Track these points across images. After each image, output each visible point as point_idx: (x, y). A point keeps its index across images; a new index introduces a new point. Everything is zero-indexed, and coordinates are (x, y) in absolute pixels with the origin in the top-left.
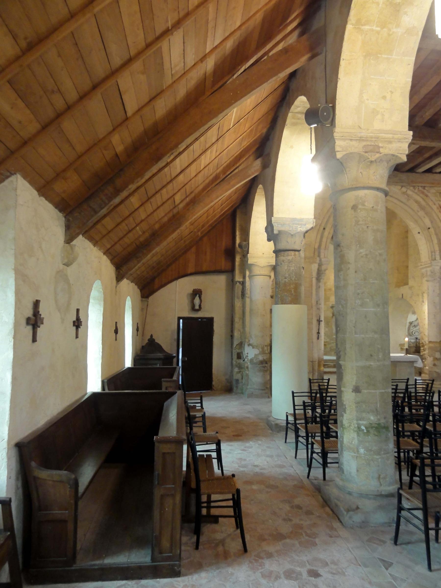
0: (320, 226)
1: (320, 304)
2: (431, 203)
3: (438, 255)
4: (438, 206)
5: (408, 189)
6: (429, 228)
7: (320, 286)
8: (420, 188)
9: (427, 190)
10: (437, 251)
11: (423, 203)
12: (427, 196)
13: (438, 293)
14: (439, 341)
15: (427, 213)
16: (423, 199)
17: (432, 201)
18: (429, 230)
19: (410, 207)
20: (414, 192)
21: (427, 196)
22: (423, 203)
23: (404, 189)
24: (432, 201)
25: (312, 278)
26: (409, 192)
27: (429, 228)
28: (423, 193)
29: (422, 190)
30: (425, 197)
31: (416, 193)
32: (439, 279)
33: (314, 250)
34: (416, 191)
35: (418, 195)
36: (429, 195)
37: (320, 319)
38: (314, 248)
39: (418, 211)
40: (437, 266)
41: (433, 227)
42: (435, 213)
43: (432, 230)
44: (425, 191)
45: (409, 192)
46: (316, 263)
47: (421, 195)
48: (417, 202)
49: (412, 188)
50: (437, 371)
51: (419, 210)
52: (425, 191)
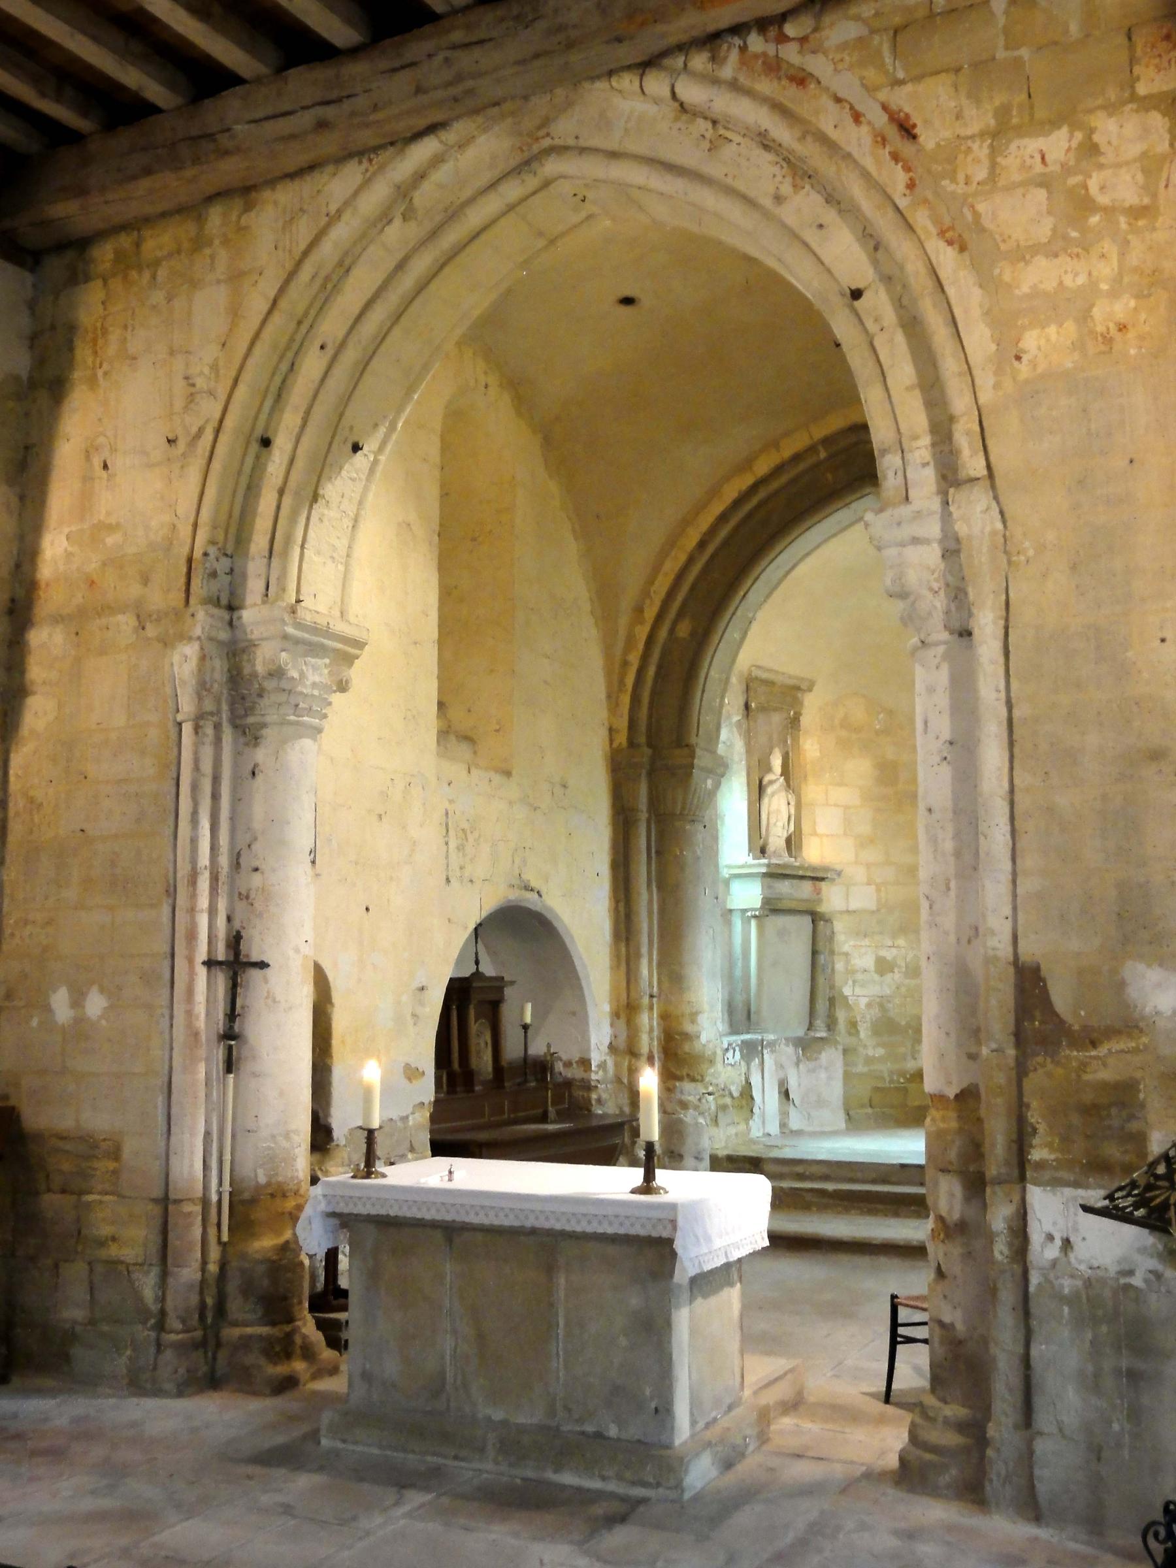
0: (217, 431)
1: (256, 870)
2: (829, 120)
3: (925, 465)
4: (881, 119)
5: (675, 73)
6: (856, 294)
7: (256, 766)
8: (756, 43)
9: (803, 40)
10: (916, 438)
11: (782, 133)
12: (801, 79)
13: (946, 735)
14: (951, 1092)
15: (831, 199)
16: (780, 109)
17: (838, 100)
18: (857, 304)
19: (730, 191)
20: (716, 81)
21: (801, 79)
22: (782, 133)
23: (657, 84)
24: (838, 100)
25: (180, 724)
26: (692, 92)
27: (856, 294)
28: (773, 67)
29: (771, 49)
30: (788, 94)
31: (734, 86)
32: (945, 636)
33: (185, 570)
34: (727, 71)
35: (749, 93)
36: (817, 65)
37: (237, 953)
38: (190, 561)
39: (778, 199)
40: (916, 541)
41: (888, 279)
42: (866, 175)
43: (878, 301)
44: (790, 53)
45: (692, 92)
46: (190, 639)
47: (765, 86)
48: (766, 142)
49: (699, 61)
50: (947, 1319)
51: (786, 189)
52: (790, 53)
